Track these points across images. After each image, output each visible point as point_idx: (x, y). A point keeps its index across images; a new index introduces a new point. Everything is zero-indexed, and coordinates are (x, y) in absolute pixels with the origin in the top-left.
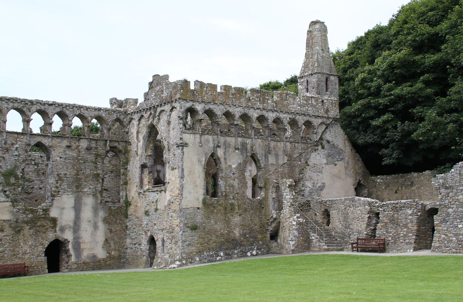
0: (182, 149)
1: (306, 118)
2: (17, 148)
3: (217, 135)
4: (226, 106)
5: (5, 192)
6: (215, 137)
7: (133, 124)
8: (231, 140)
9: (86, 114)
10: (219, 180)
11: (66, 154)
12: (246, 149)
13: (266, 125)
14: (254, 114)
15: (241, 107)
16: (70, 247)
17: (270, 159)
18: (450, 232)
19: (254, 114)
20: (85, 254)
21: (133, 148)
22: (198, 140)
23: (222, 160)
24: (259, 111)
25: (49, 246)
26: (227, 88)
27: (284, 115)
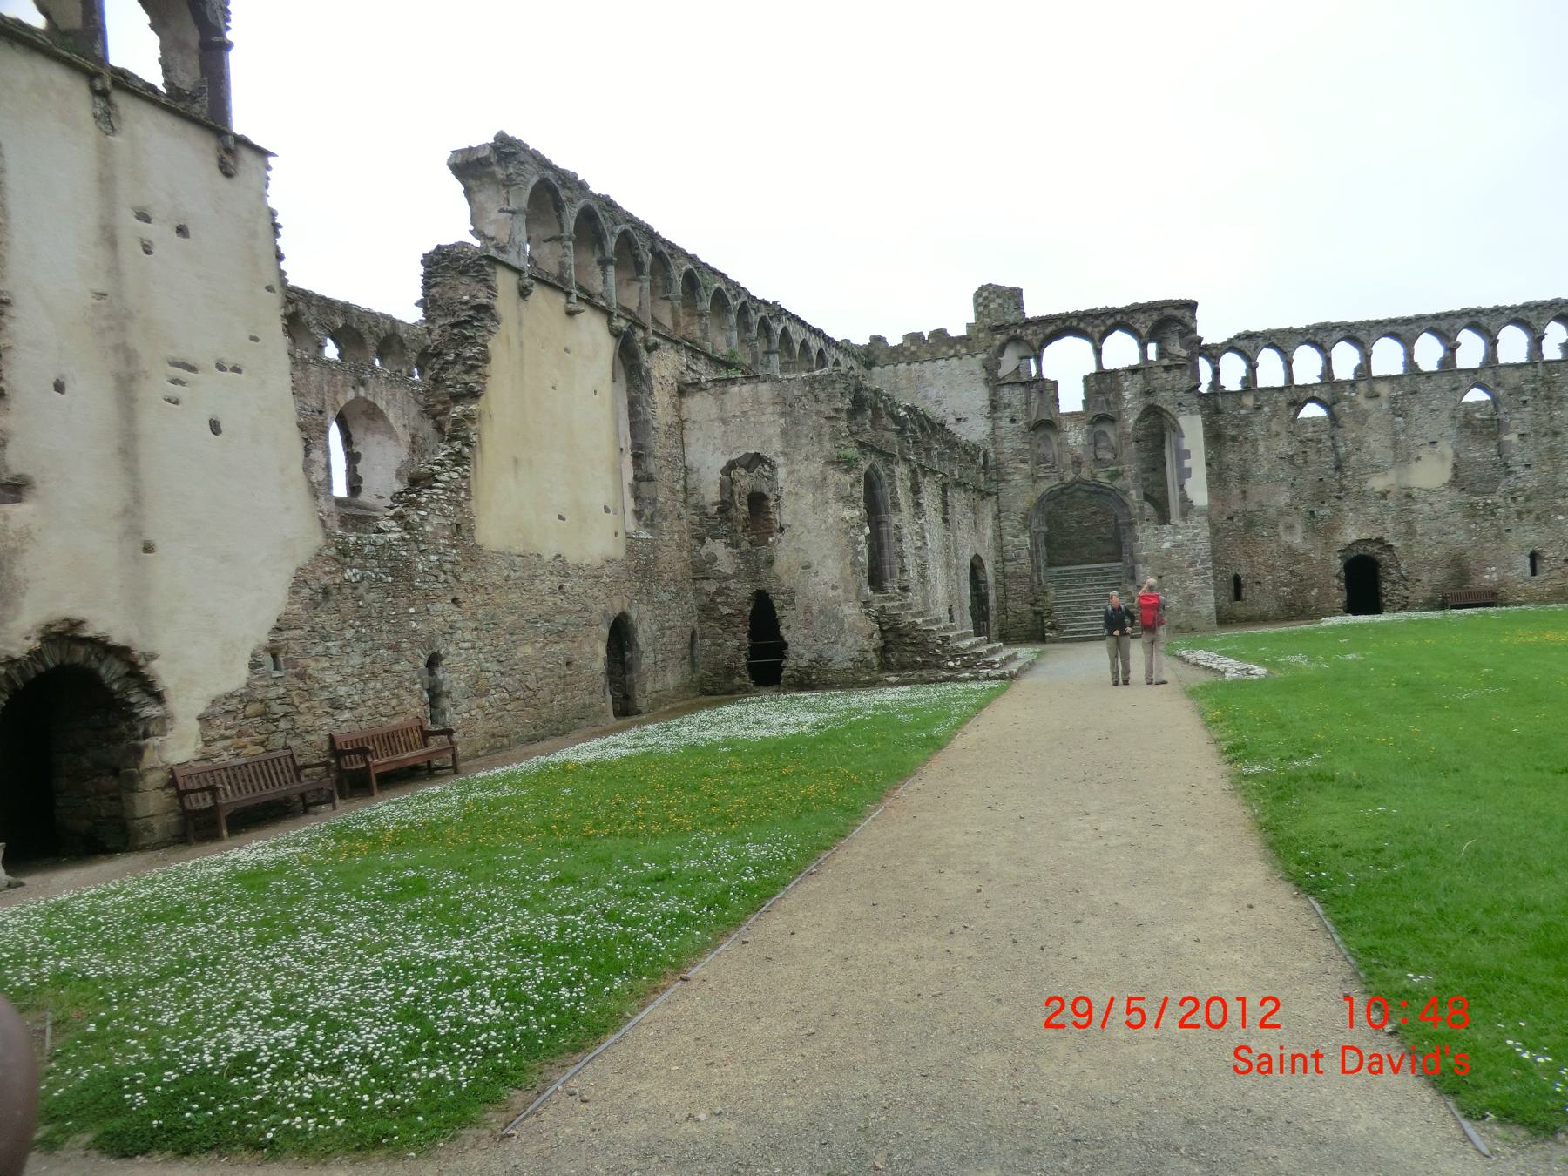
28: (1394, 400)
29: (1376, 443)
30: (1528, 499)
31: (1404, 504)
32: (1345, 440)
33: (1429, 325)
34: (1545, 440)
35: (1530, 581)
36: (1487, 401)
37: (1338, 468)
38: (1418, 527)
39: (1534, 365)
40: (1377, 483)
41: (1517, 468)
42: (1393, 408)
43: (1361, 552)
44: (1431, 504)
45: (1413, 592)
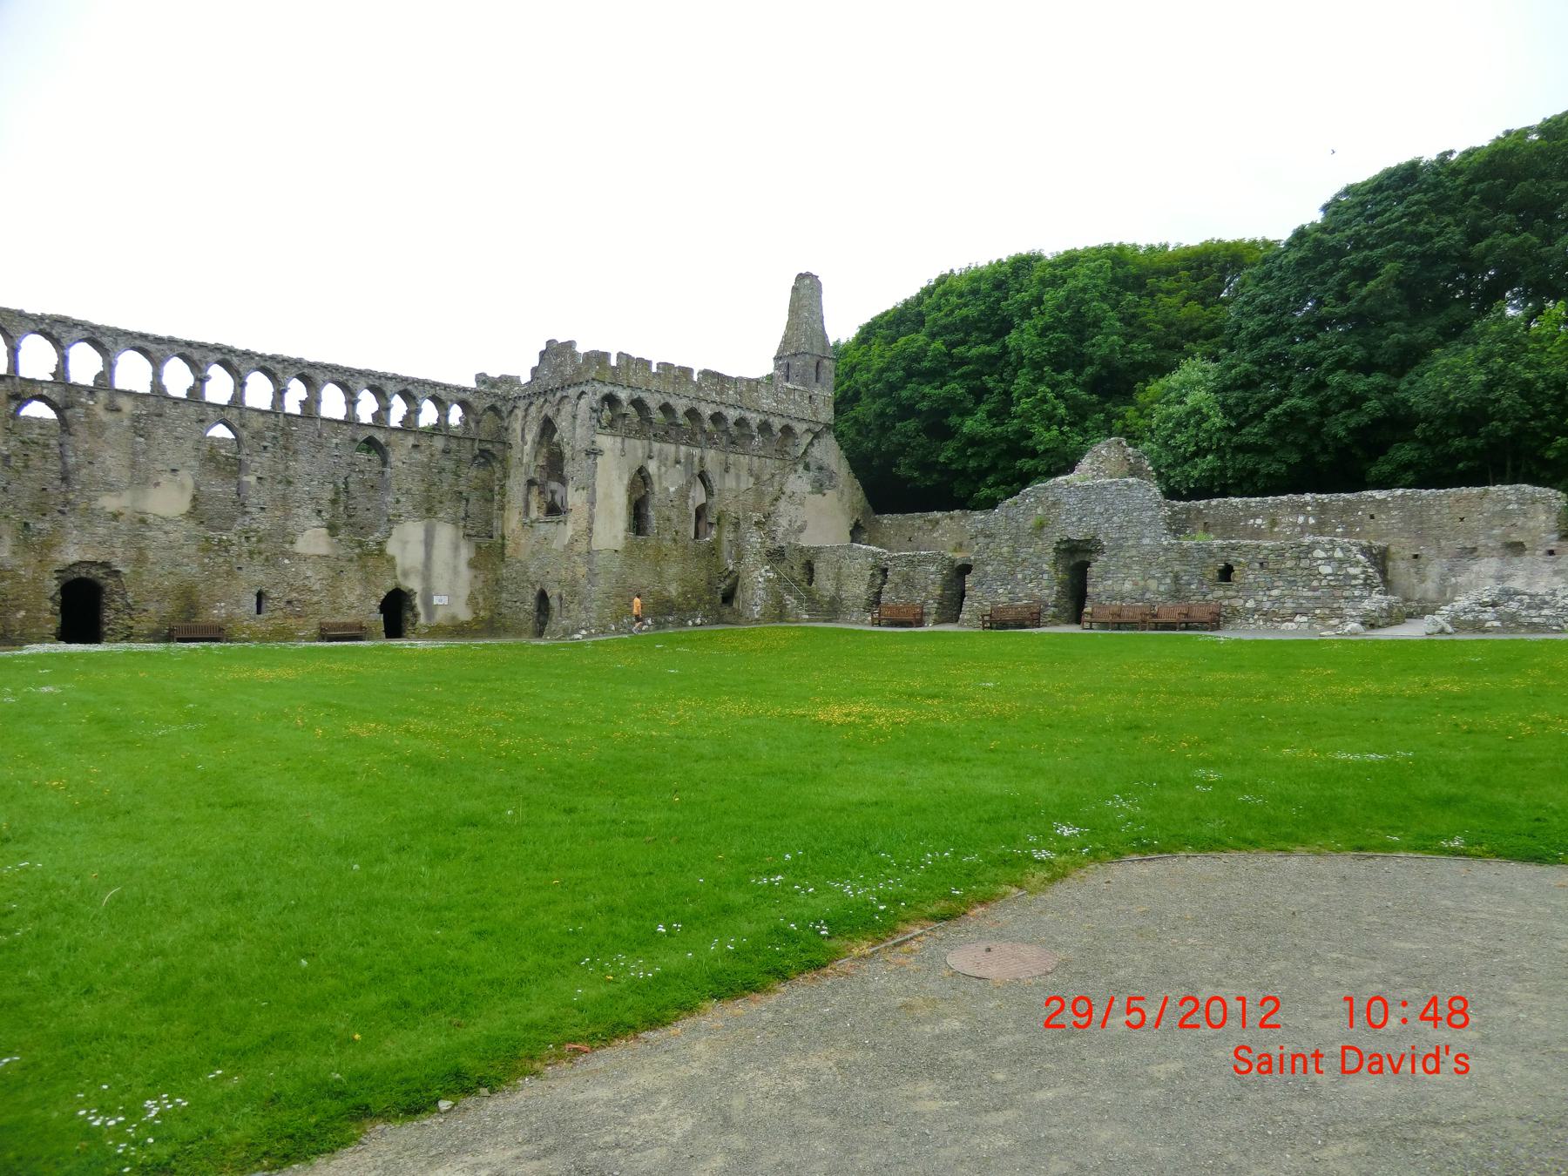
0: (595, 459)
1: (785, 421)
3: (649, 439)
4: (665, 395)
5: (320, 511)
6: (646, 442)
7: (516, 415)
8: (670, 449)
9: (442, 394)
10: (650, 509)
11: (410, 458)
12: (692, 463)
13: (724, 428)
14: (707, 411)
16: (418, 601)
17: (727, 480)
18: (987, 600)
19: (707, 411)
21: (514, 454)
22: (619, 445)
23: (655, 479)
24: (714, 406)
25: (384, 600)
26: (666, 367)
28: (136, 419)
29: (113, 460)
30: (259, 541)
31: (137, 529)
32: (75, 450)
33: (182, 350)
34: (279, 487)
35: (255, 620)
36: (208, 430)
37: (64, 479)
38: (150, 555)
39: (277, 415)
40: (109, 503)
41: (253, 510)
43: (84, 575)
44: (166, 533)
45: (138, 622)
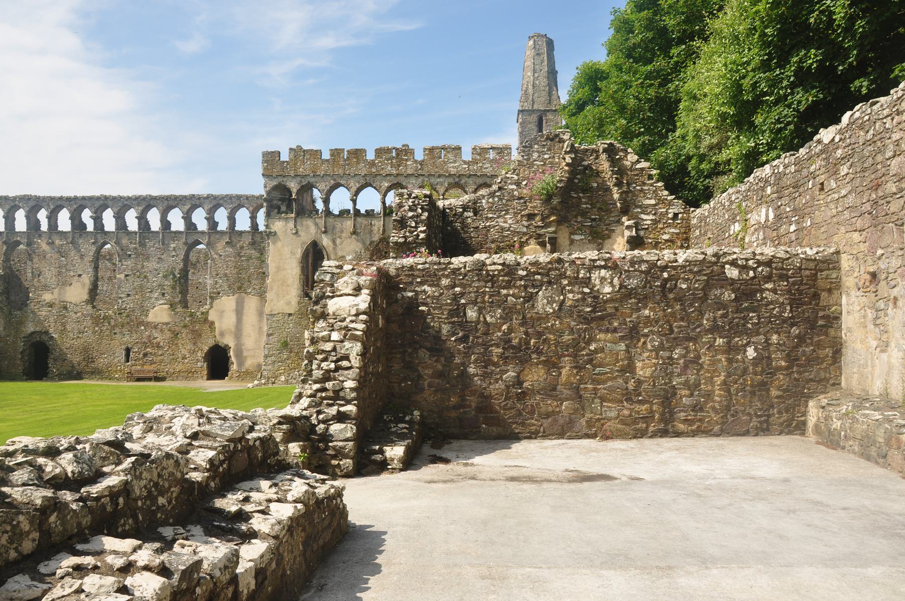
2: (174, 248)
15: (359, 177)
16: (232, 353)
20: (249, 363)
27: (438, 180)
40: (47, 297)
42: (60, 252)
